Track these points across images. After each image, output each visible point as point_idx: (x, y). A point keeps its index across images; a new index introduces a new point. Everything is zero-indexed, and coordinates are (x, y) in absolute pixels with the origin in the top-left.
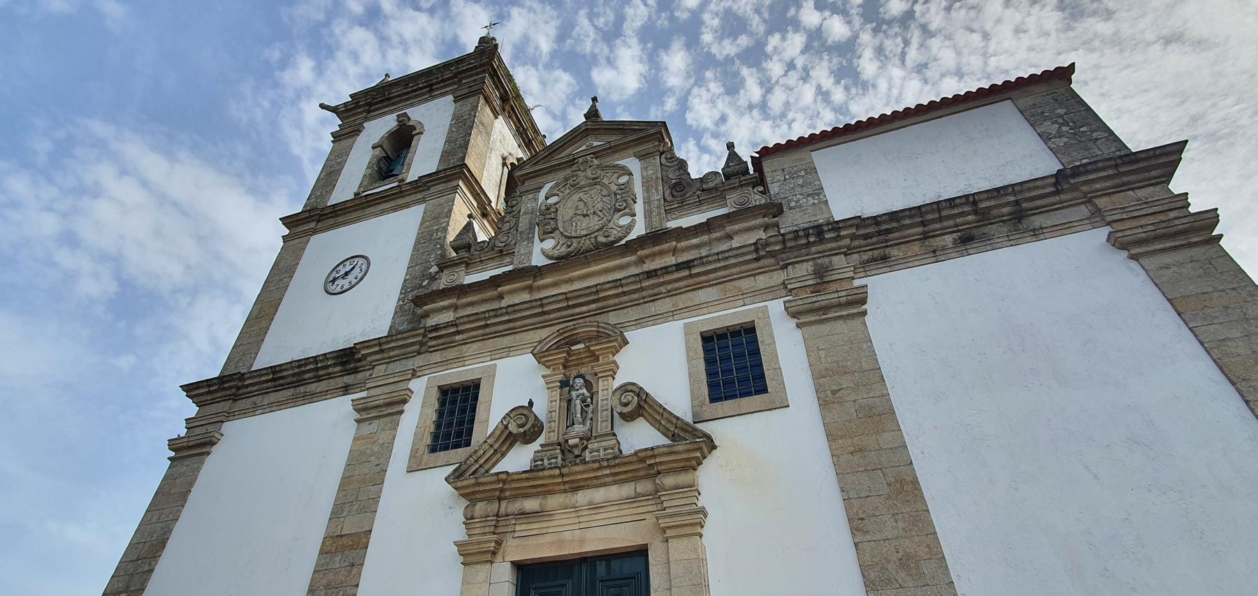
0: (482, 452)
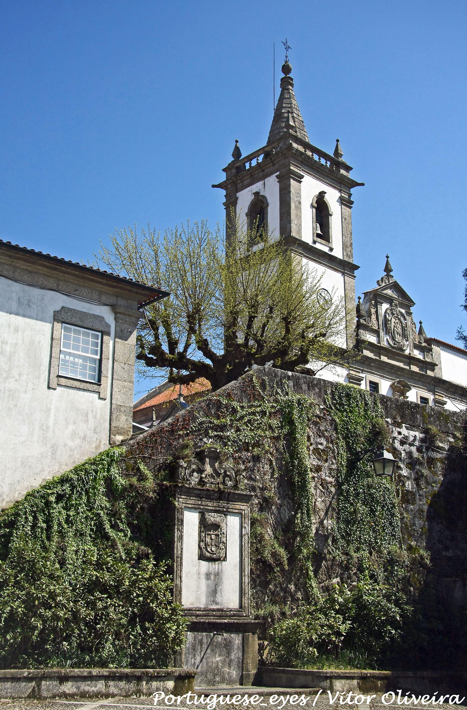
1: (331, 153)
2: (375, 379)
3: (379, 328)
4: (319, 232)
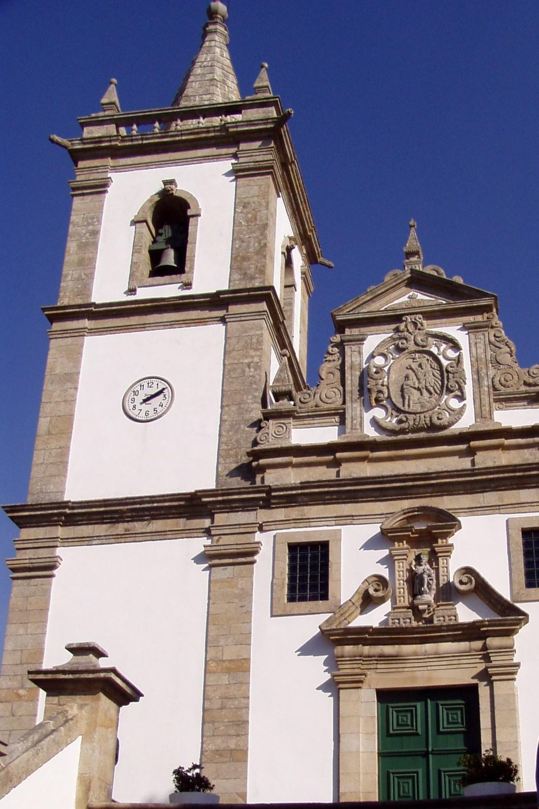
0: (347, 608)
3: (344, 403)
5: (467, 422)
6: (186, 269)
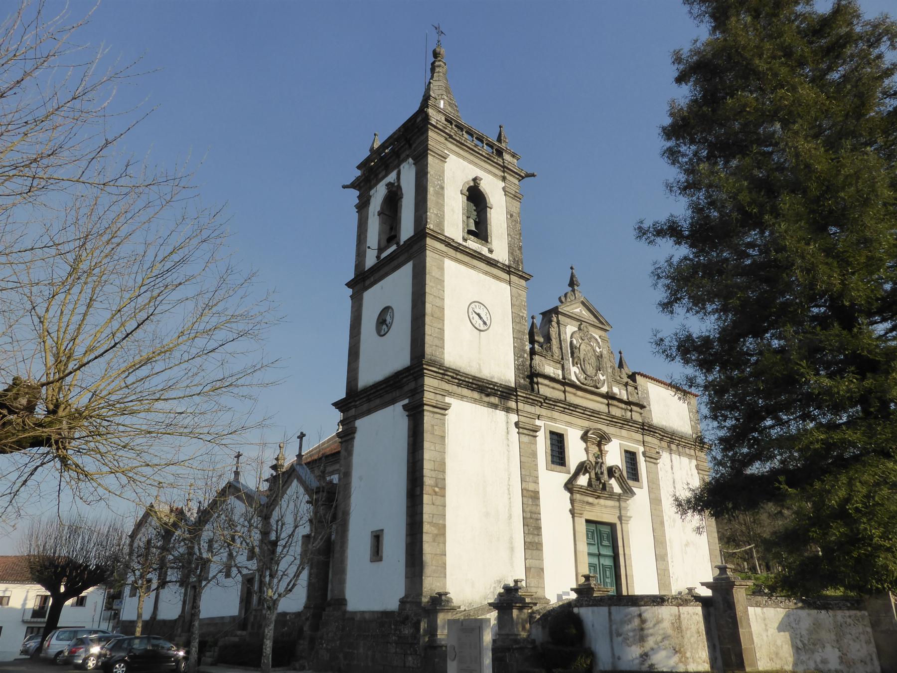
1: (493, 139)
2: (559, 427)
4: (473, 228)
5: (604, 389)
6: (489, 240)
